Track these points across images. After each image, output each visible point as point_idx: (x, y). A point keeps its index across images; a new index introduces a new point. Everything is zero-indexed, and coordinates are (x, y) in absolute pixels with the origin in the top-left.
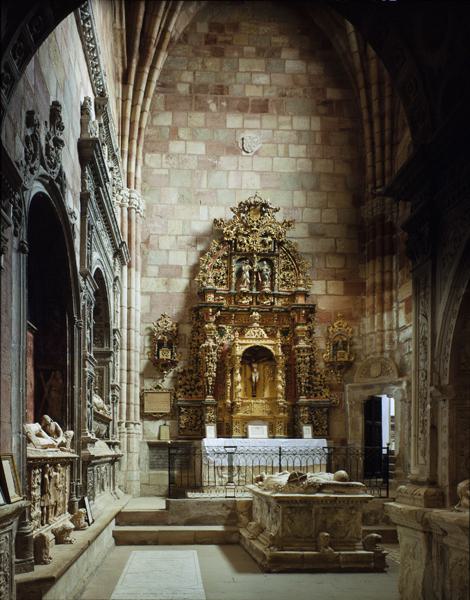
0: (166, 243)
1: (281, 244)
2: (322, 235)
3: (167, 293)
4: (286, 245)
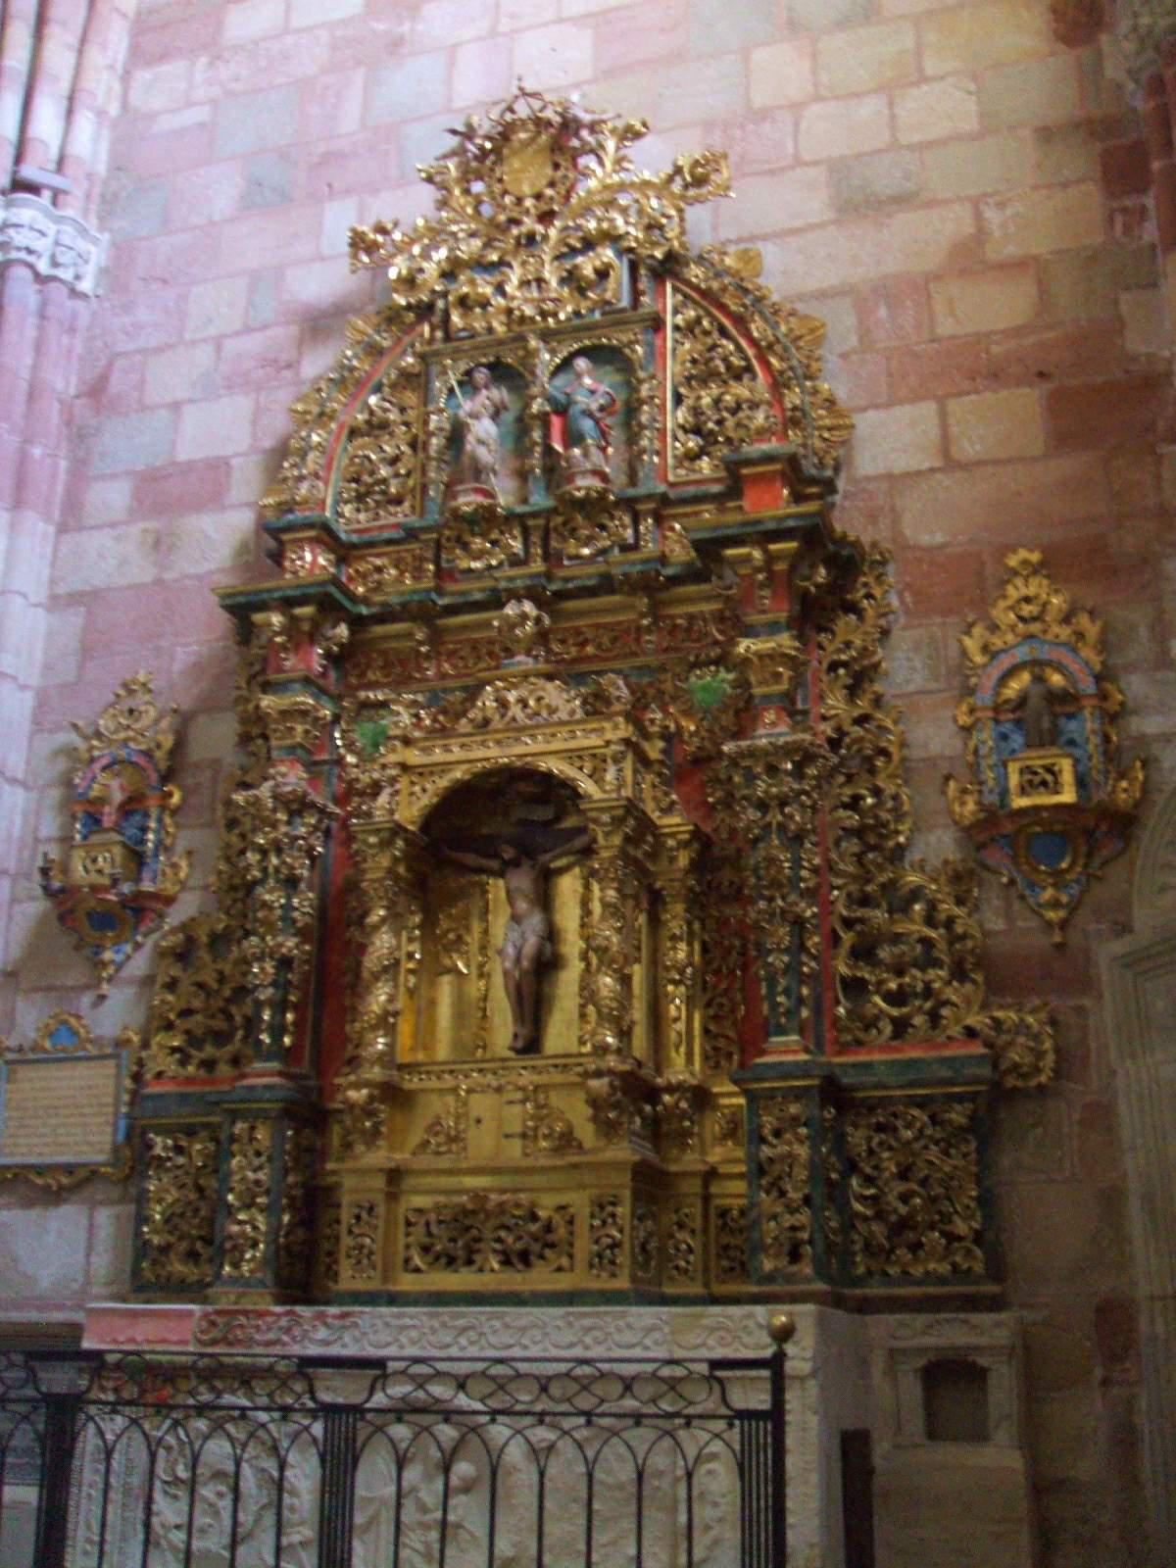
0: (169, 378)
1: (669, 267)
2: (902, 201)
3: (158, 582)
4: (695, 273)
